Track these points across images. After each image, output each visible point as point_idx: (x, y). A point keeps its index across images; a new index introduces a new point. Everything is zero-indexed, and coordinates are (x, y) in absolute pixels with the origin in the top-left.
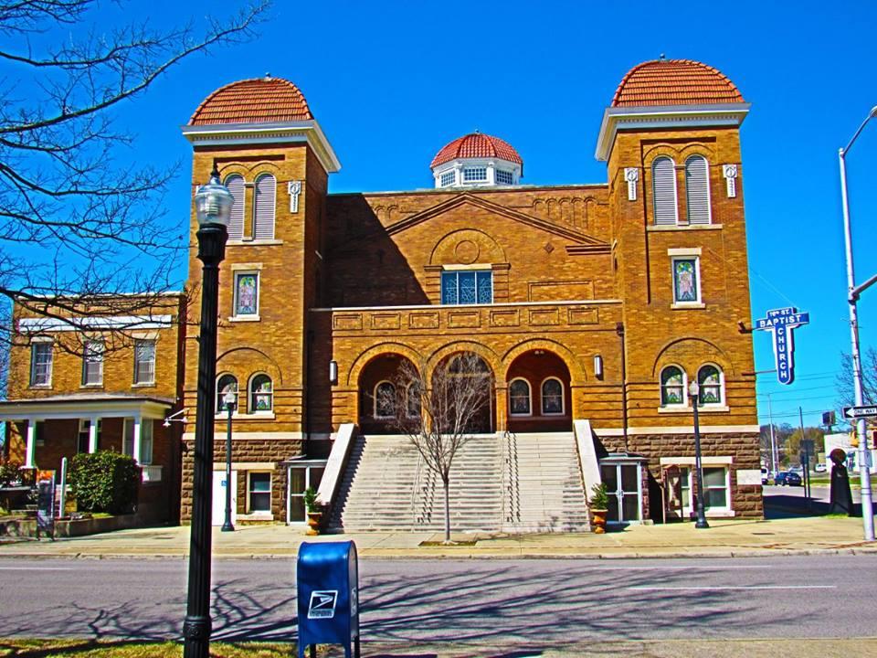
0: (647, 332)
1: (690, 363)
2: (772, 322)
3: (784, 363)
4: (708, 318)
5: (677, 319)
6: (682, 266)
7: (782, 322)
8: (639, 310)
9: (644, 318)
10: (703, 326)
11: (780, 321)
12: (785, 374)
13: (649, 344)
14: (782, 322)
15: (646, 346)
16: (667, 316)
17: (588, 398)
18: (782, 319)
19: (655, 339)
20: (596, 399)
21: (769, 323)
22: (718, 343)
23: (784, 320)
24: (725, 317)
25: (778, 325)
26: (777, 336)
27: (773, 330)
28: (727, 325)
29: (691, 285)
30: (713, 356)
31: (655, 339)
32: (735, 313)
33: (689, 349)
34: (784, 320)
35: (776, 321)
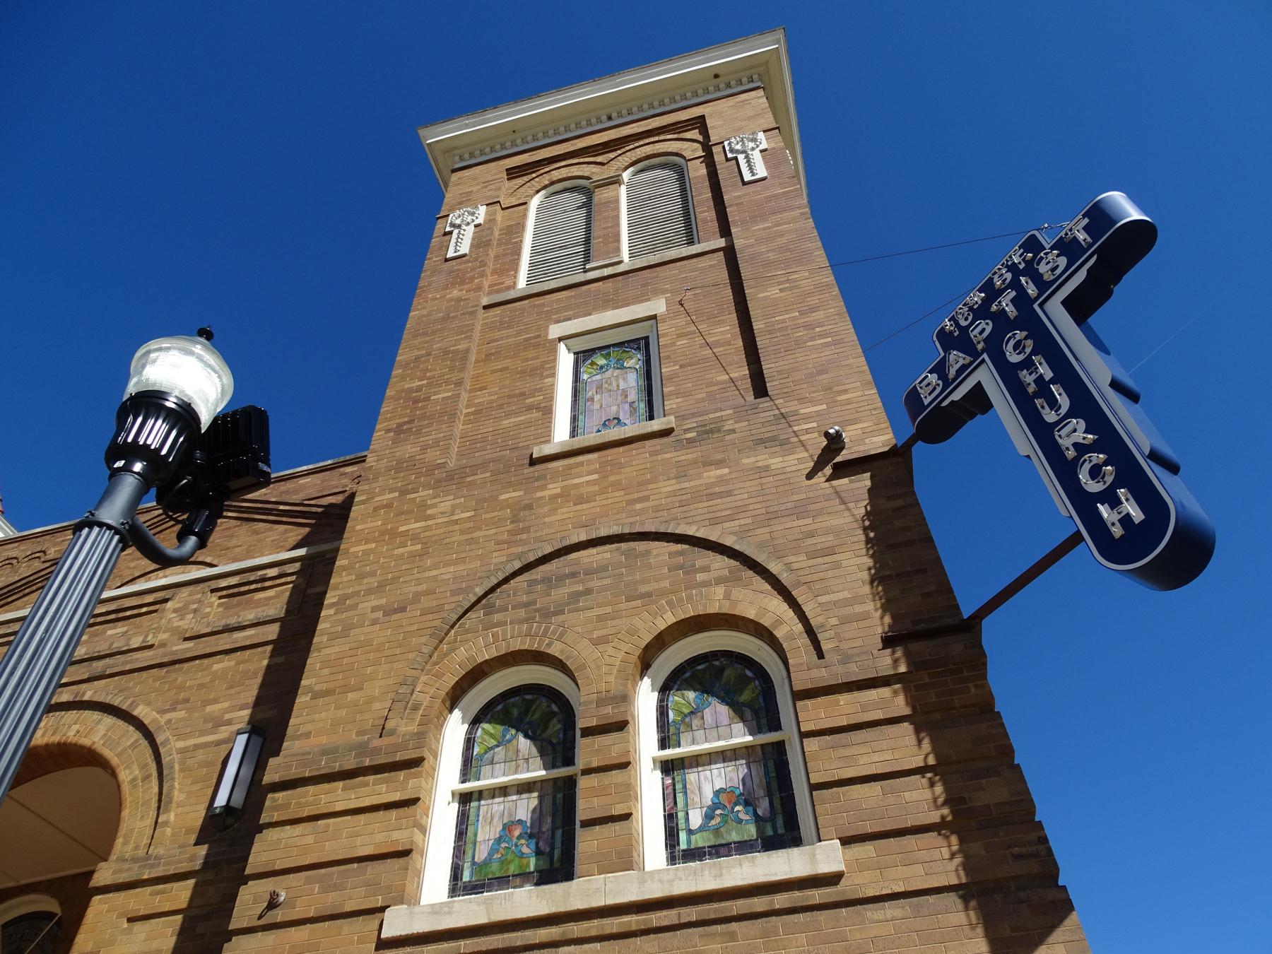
0: (421, 555)
1: (596, 642)
4: (686, 456)
5: (554, 488)
6: (602, 361)
8: (403, 492)
9: (421, 512)
10: (668, 486)
13: (417, 597)
15: (403, 609)
16: (510, 486)
19: (447, 572)
22: (742, 534)
24: (762, 441)
28: (775, 462)
29: (633, 396)
30: (720, 591)
31: (447, 572)
32: (807, 418)
33: (595, 583)
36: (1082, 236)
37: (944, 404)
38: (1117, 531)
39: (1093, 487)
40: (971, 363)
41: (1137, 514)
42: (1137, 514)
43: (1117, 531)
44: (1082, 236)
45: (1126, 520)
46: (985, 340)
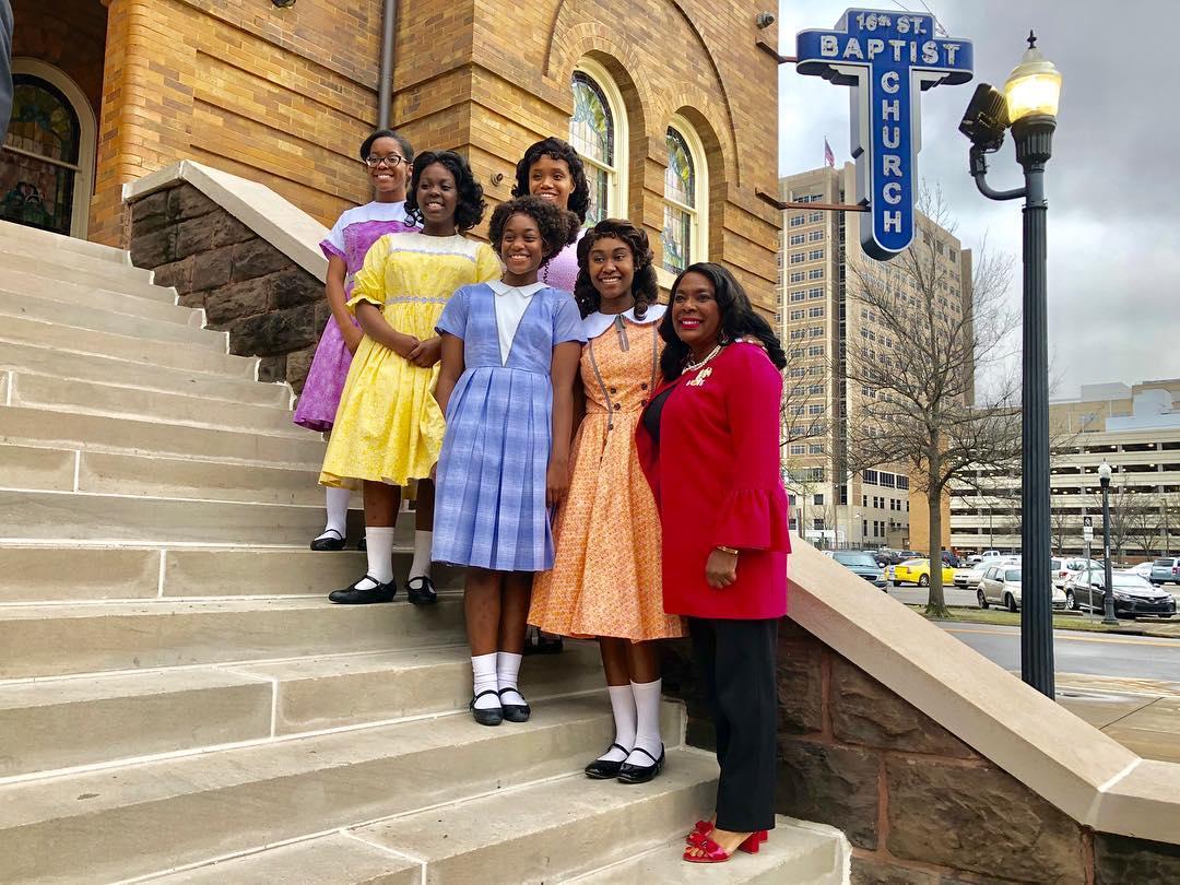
2: (864, 49)
3: (897, 187)
7: (897, 52)
11: (889, 49)
12: (898, 222)
14: (897, 52)
17: (217, 84)
18: (898, 44)
20: (259, 111)
21: (853, 46)
23: (905, 51)
25: (881, 64)
26: (878, 95)
27: (863, 74)
34: (905, 51)
35: (876, 46)
36: (951, 56)
37: (832, 67)
38: (887, 228)
39: (888, 198)
40: (859, 60)
41: (898, 230)
42: (898, 230)
43: (887, 228)
44: (951, 56)
45: (893, 226)
46: (875, 54)
